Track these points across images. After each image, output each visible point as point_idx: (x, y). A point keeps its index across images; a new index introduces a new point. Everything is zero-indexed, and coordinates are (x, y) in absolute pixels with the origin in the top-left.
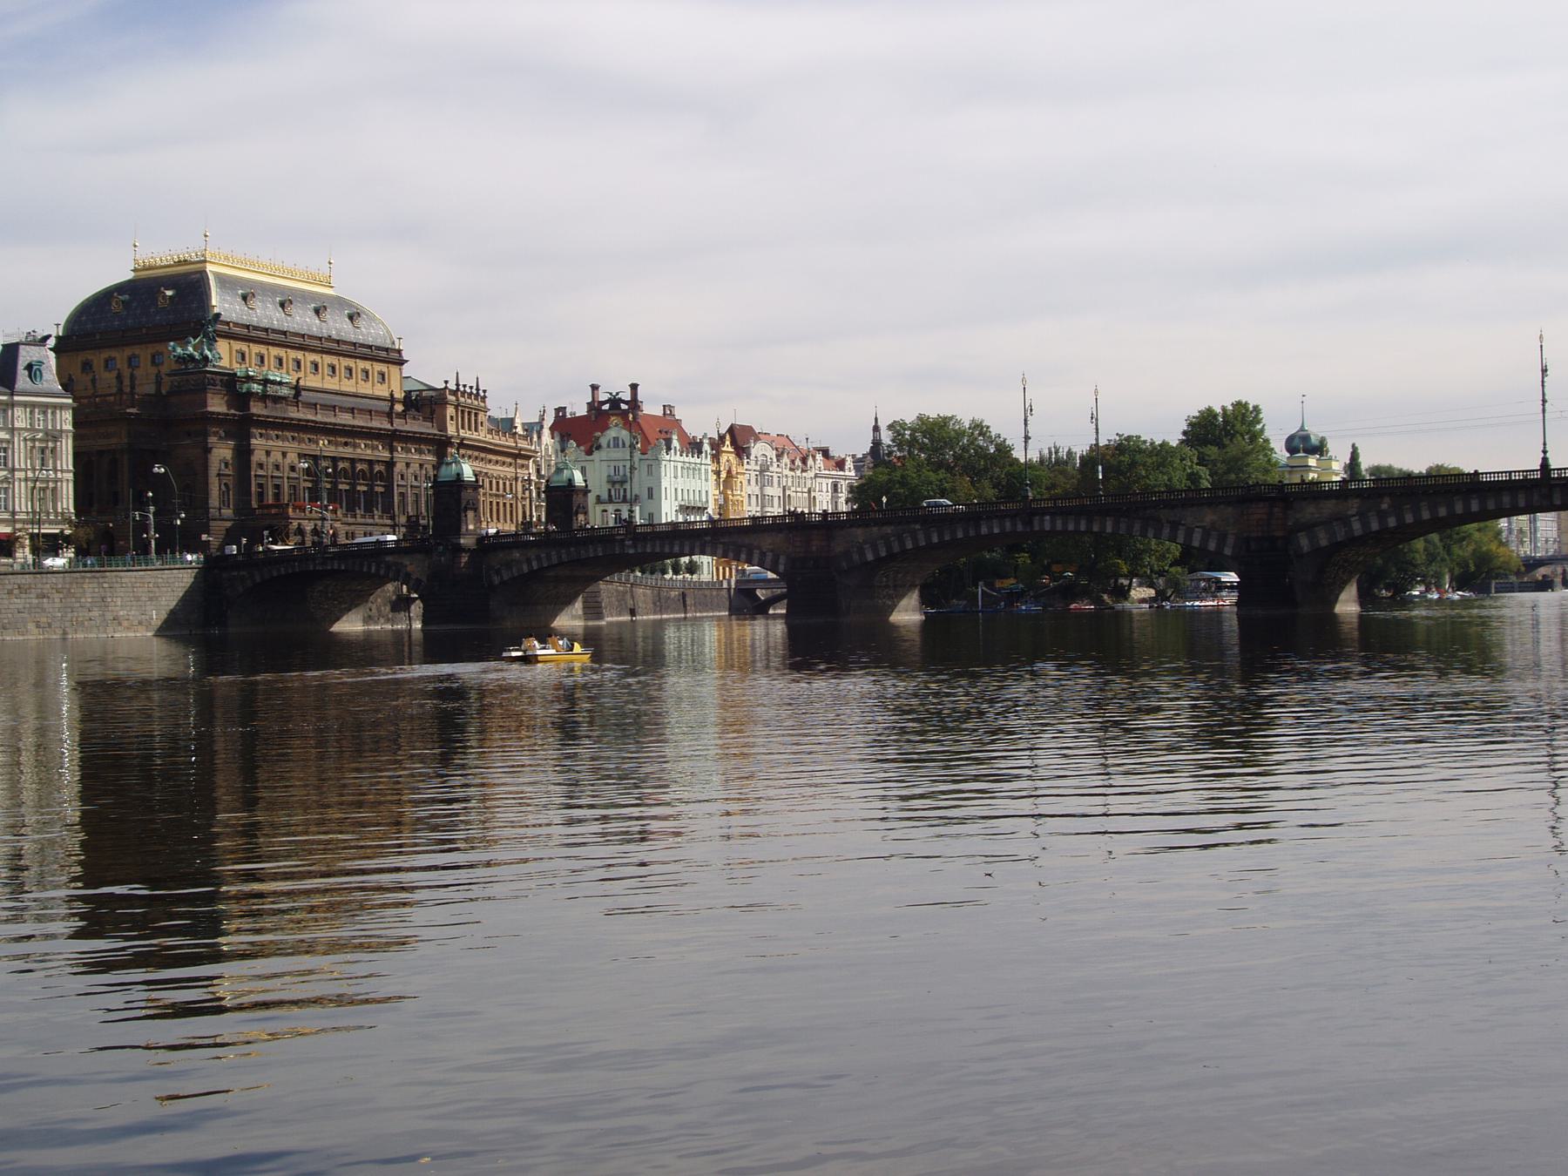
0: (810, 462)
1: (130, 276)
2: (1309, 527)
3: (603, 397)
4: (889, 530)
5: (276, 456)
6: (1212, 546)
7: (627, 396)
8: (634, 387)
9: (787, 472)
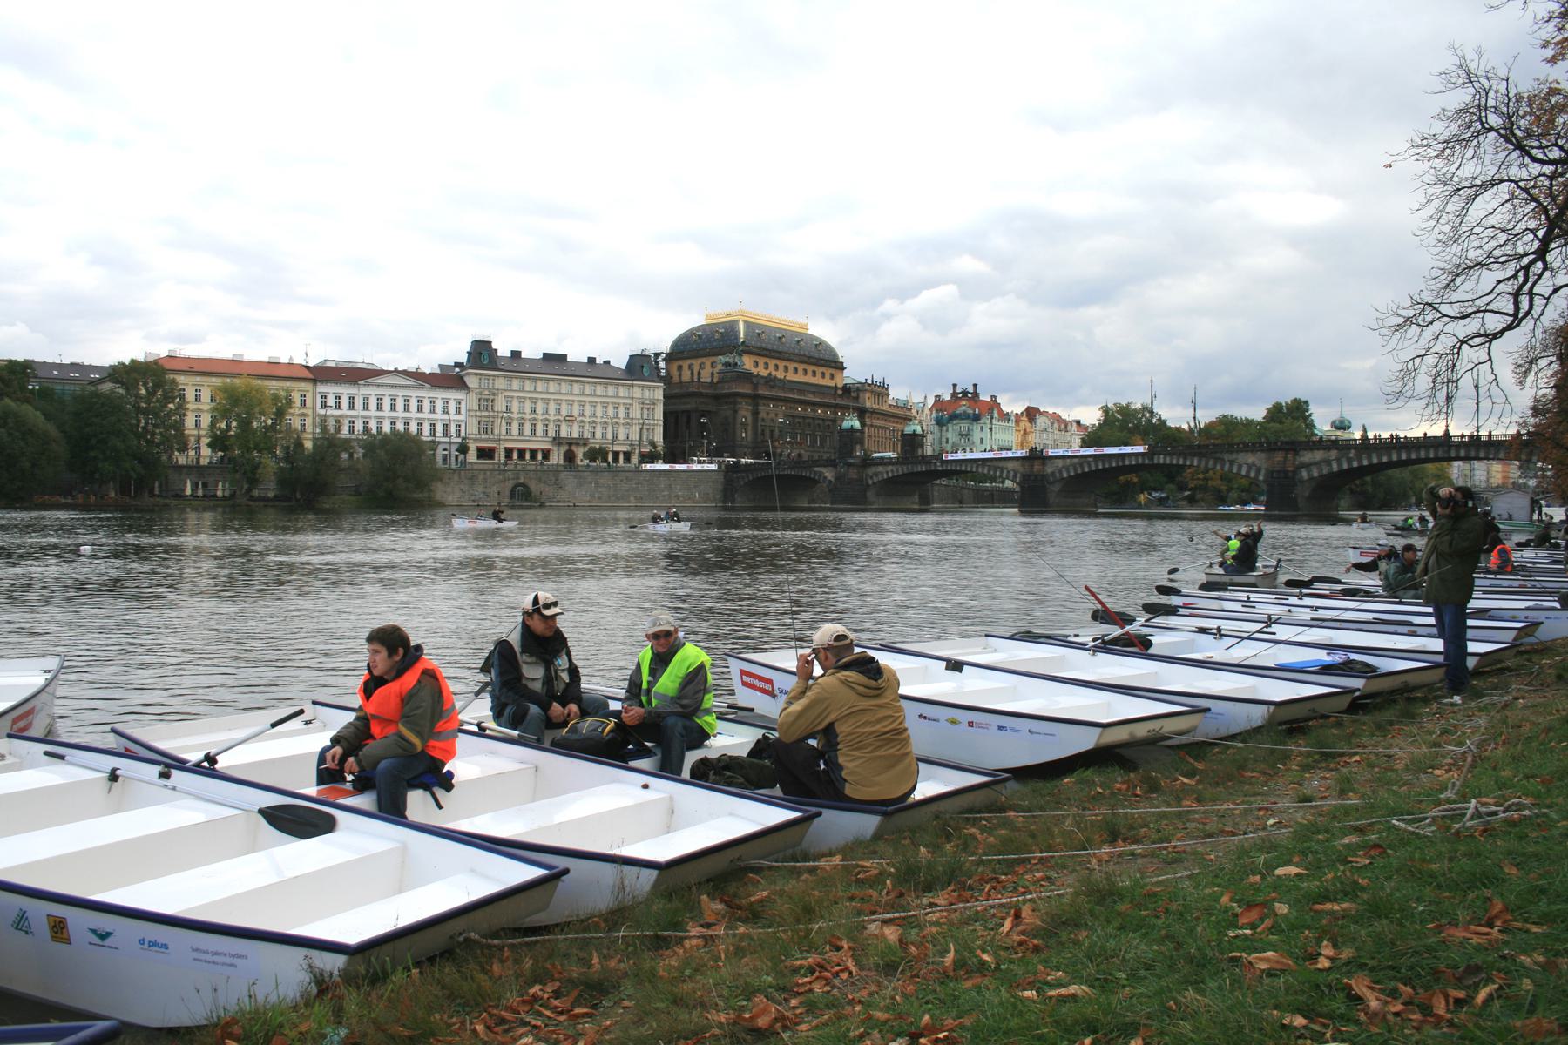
2: (1307, 466)
6: (1252, 474)
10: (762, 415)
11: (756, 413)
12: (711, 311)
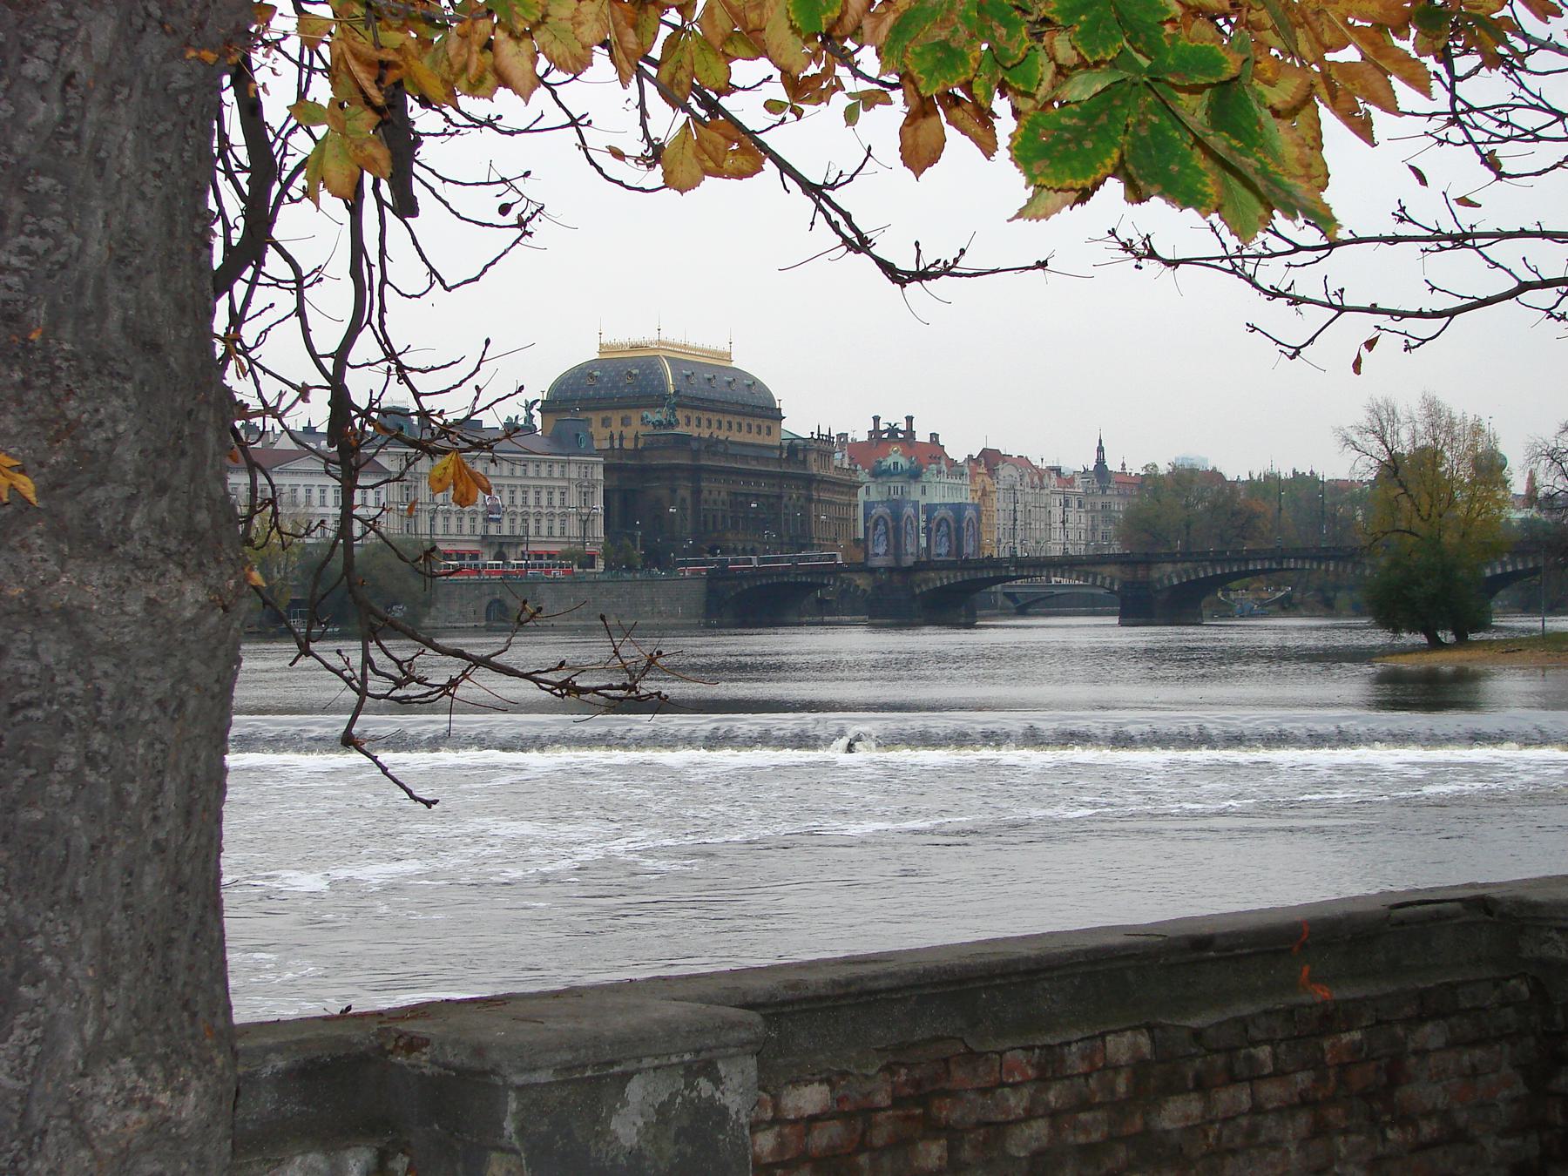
0: (1046, 481)
1: (597, 356)
3: (883, 427)
4: (1188, 565)
5: (715, 495)
7: (903, 427)
8: (909, 419)
9: (1028, 490)
10: (705, 494)
11: (697, 492)
12: (606, 340)
